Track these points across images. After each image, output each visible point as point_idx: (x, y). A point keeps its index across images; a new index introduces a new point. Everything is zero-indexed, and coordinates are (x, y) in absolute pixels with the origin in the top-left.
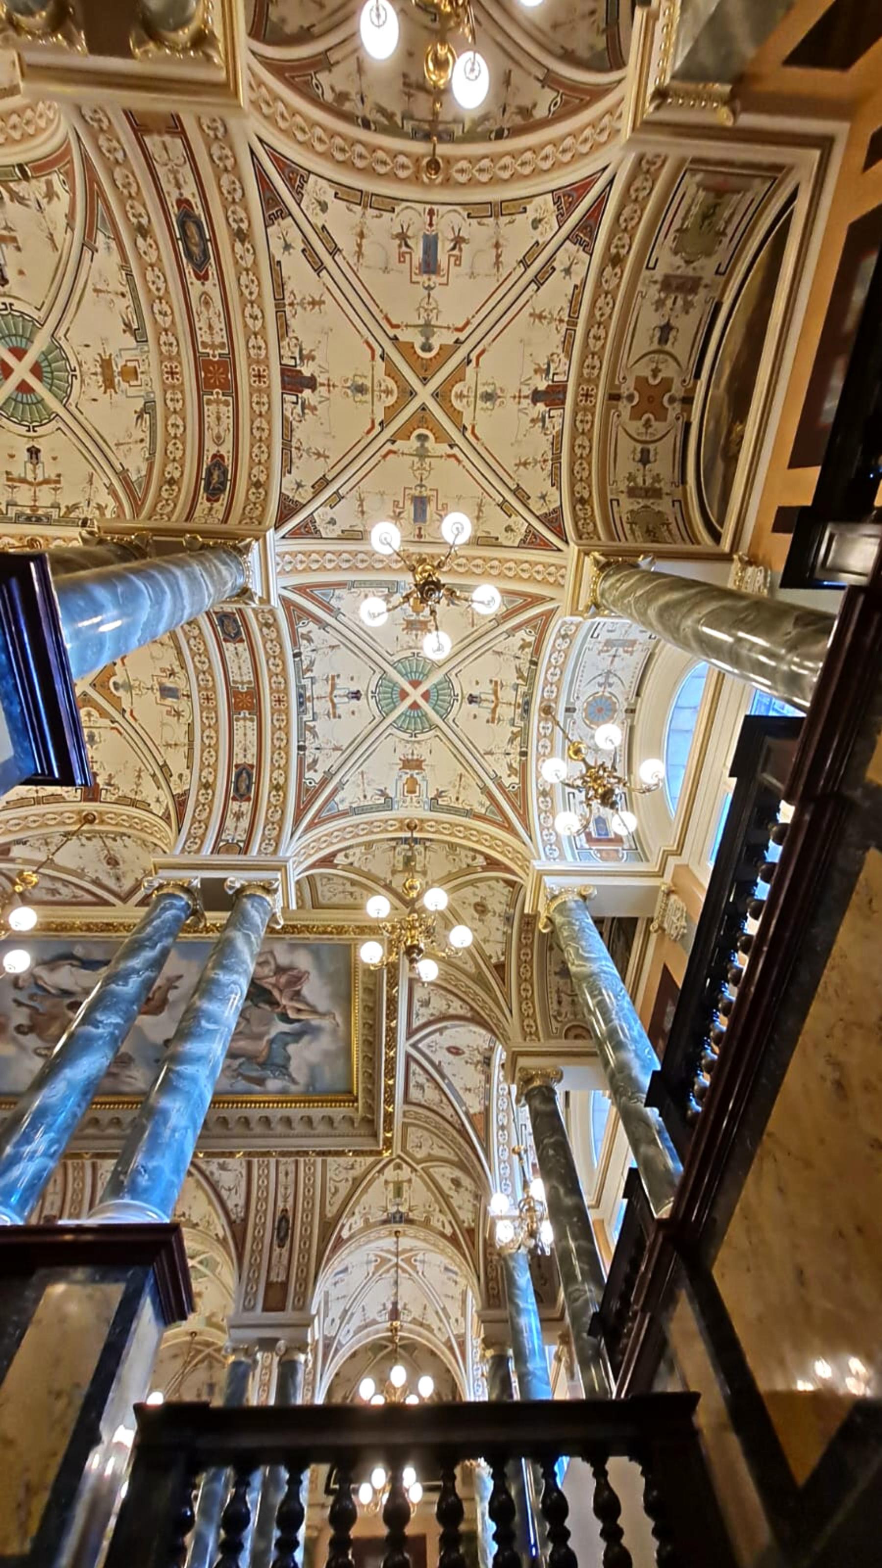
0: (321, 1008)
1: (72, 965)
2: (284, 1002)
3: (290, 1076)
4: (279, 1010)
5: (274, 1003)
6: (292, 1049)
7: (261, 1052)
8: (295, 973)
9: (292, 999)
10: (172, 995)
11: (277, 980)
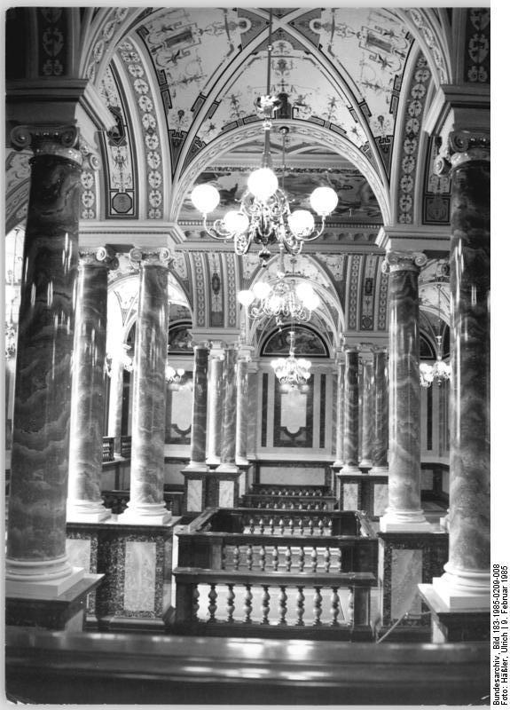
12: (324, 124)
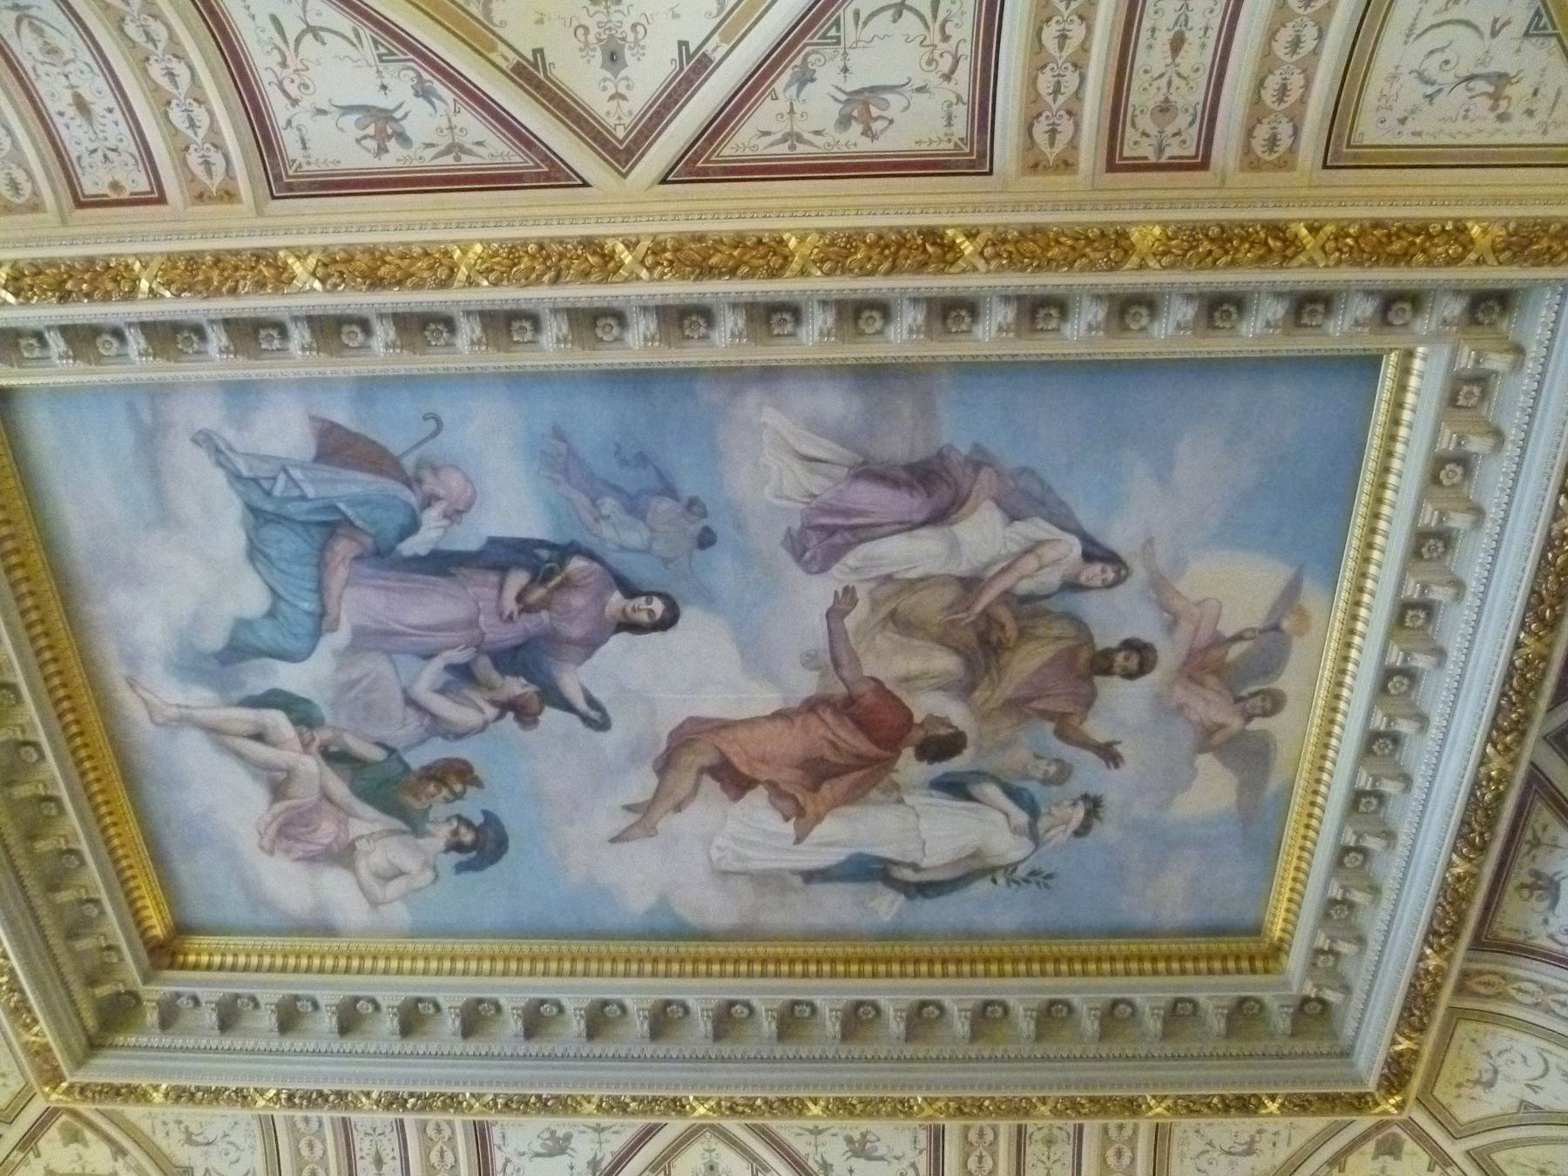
1: (915, 867)
2: (310, 765)
3: (235, 477)
4: (322, 735)
5: (336, 757)
6: (250, 597)
7: (348, 583)
8: (299, 849)
9: (290, 772)
10: (642, 784)
11: (342, 823)
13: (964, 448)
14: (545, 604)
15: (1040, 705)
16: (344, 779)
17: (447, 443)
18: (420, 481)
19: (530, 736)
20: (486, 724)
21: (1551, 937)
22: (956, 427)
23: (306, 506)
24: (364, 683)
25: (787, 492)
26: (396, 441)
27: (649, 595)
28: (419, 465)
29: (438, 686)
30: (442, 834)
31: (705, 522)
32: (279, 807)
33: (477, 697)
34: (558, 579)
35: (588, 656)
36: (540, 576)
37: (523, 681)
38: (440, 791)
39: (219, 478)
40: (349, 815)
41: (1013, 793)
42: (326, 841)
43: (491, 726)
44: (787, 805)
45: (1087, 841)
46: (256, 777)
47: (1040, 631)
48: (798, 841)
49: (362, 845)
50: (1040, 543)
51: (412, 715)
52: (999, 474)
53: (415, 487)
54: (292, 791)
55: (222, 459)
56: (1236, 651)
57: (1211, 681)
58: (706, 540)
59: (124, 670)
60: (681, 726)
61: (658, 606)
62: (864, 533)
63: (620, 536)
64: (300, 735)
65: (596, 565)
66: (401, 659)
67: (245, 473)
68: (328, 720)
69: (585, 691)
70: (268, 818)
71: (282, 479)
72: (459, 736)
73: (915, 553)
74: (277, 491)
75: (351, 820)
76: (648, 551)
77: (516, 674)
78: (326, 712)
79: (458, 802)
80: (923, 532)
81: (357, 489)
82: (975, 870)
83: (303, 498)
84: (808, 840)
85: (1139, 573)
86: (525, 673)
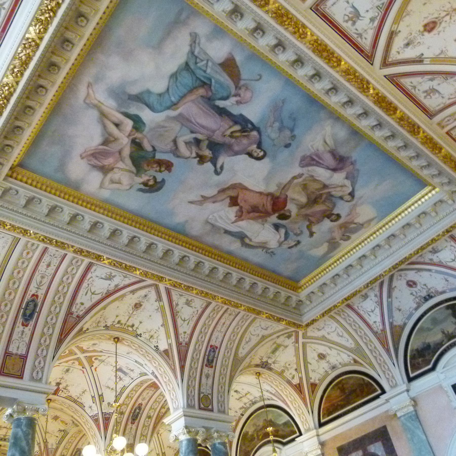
0: (94, 114)
1: (251, 240)
2: (125, 141)
4: (138, 135)
5: (136, 144)
7: (193, 101)
8: (94, 162)
9: (116, 139)
11: (117, 162)
12: (75, 401)
13: (353, 159)
14: (236, 138)
15: (310, 218)
16: (131, 150)
17: (258, 85)
18: (240, 89)
19: (199, 167)
20: (189, 157)
21: (358, 307)
22: (357, 154)
23: (203, 74)
24: (166, 129)
25: (314, 146)
26: (245, 74)
27: (262, 150)
28: (243, 85)
29: (187, 141)
30: (145, 178)
31: (291, 142)
32: (101, 147)
33: (194, 149)
34: (246, 134)
35: (233, 156)
36: (243, 130)
37: (211, 152)
38: (157, 167)
39: (186, 49)
40: (121, 160)
41: (286, 234)
42: (106, 164)
43: (190, 159)
44: (239, 213)
45: (289, 250)
46: (103, 135)
47: (326, 203)
48: (233, 223)
49: (115, 170)
50: (345, 186)
51: (172, 144)
52: (354, 168)
53: (237, 89)
54: (110, 145)
55: (194, 45)
56: (353, 226)
57: (343, 229)
58: (287, 146)
59: (91, 81)
60: (236, 184)
61: (261, 154)
62: (318, 164)
63: (271, 133)
64: (131, 131)
65: (258, 136)
66: (184, 128)
67: (196, 53)
68: (145, 133)
69: (223, 163)
70: (93, 148)
71: (205, 62)
72: (178, 157)
73: (322, 174)
74: (199, 65)
75: (121, 163)
76: (273, 140)
77: (210, 150)
78: (147, 129)
79: (159, 173)
80: (329, 171)
81: (222, 79)
82: (263, 246)
83: (205, 71)
84: (236, 224)
85: (354, 202)
86: (211, 150)
